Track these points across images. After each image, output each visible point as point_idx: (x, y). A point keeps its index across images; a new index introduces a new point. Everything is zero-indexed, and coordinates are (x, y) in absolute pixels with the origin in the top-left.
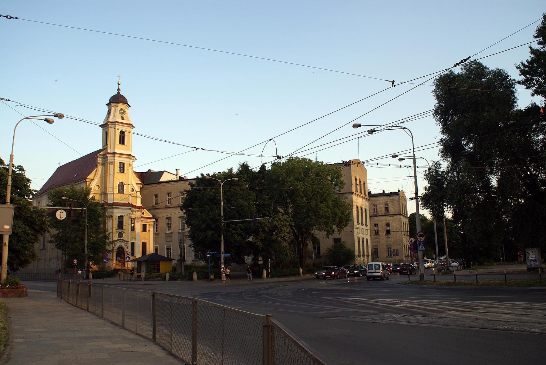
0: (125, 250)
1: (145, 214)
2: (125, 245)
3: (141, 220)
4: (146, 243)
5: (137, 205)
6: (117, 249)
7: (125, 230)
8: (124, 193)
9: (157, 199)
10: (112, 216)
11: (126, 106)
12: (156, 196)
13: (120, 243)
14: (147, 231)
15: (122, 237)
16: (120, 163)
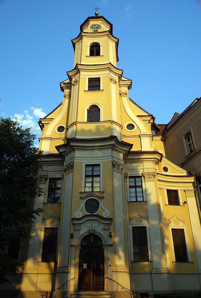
0: (104, 243)
2: (104, 230)
3: (159, 178)
4: (183, 230)
5: (142, 151)
8: (102, 119)
9: (191, 142)
10: (72, 164)
11: (101, 21)
12: (188, 136)
13: (89, 225)
16: (91, 80)
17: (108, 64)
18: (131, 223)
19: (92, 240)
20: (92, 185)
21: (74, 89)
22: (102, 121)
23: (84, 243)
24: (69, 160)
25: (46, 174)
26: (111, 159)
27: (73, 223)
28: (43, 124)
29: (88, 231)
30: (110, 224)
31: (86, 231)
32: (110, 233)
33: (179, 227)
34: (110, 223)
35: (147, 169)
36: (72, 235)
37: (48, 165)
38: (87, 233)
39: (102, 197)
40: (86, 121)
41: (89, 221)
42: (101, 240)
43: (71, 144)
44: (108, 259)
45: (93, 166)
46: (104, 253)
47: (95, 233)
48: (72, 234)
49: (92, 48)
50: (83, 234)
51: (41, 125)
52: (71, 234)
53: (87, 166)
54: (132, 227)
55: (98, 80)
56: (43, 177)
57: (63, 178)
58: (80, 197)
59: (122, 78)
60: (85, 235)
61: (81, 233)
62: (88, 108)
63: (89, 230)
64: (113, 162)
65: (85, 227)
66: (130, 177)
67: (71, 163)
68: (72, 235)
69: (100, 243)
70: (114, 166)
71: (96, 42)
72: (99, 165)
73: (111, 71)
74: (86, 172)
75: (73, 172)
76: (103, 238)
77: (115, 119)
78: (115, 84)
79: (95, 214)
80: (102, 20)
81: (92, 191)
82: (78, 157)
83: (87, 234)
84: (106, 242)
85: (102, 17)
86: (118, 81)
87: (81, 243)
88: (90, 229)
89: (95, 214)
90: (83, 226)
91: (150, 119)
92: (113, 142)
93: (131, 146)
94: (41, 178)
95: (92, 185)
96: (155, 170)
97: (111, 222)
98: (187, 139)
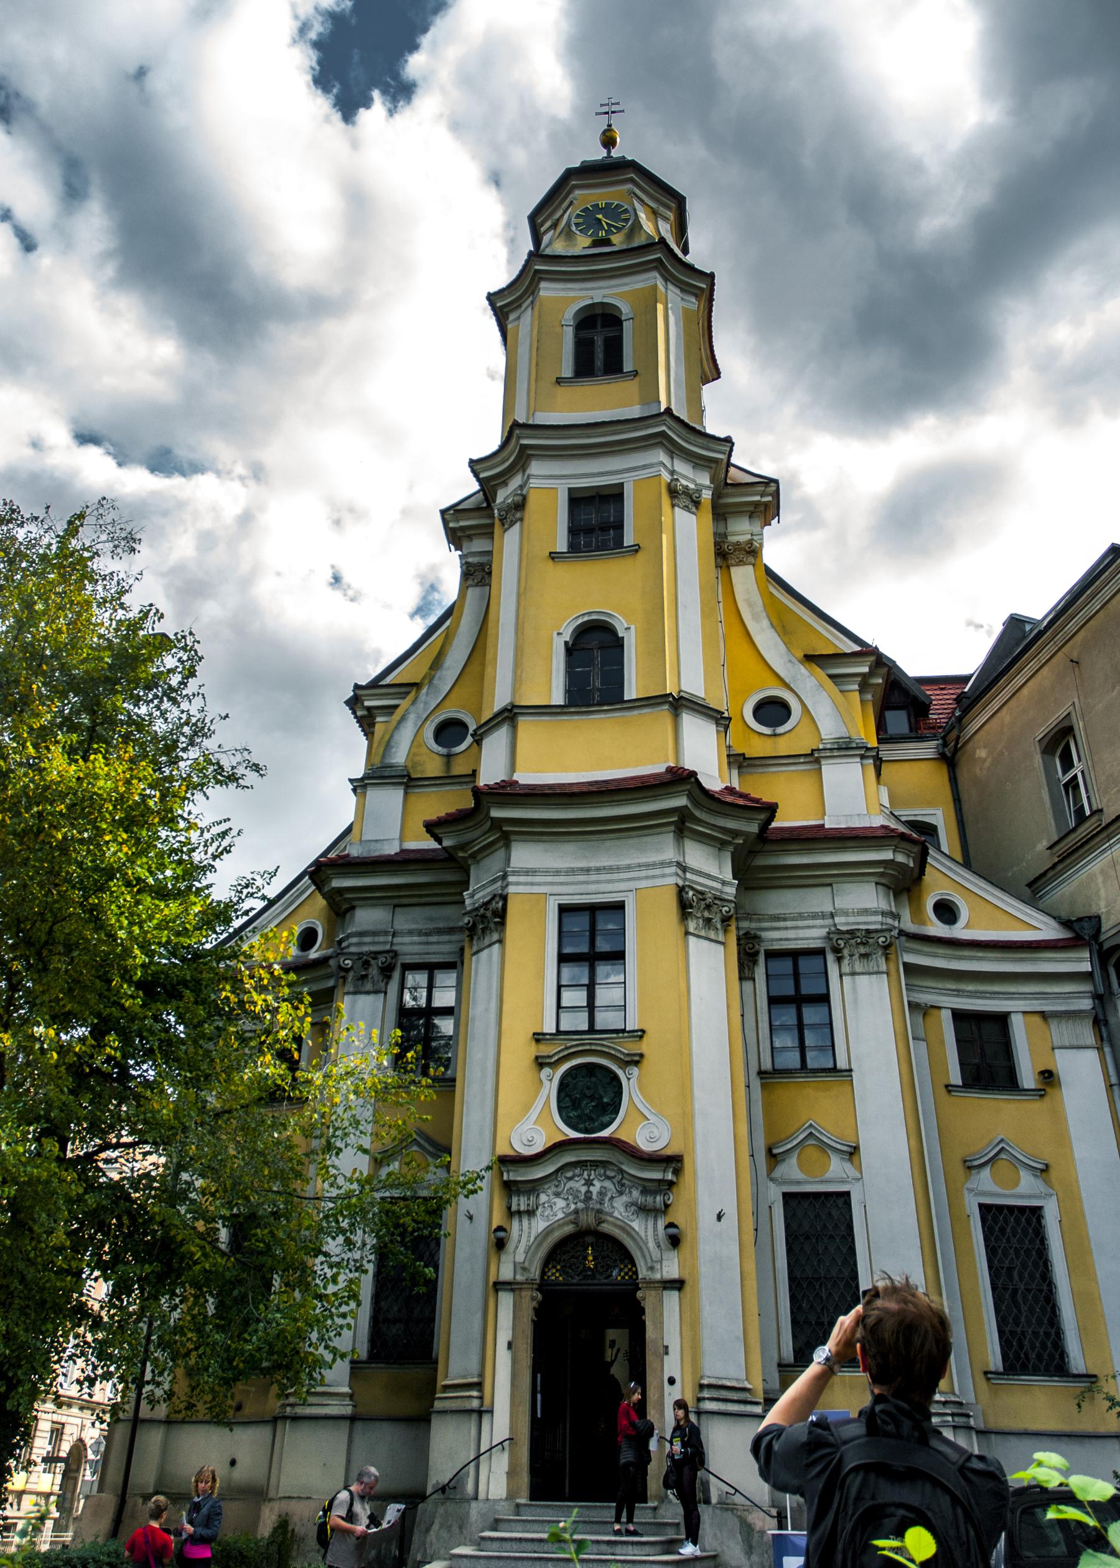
0: (643, 1273)
1: (964, 915)
2: (644, 1210)
4: (1036, 1213)
6: (551, 1259)
7: (640, 1034)
8: (631, 692)
11: (630, 186)
13: (578, 1185)
14: (1028, 1078)
15: (616, 1111)
17: (660, 419)
18: (779, 1172)
19: (591, 1258)
20: (591, 997)
21: (509, 543)
22: (634, 697)
23: (554, 1275)
24: (484, 887)
25: (388, 947)
26: (672, 880)
27: (505, 1177)
28: (369, 709)
29: (572, 1217)
30: (671, 1184)
31: (560, 1215)
32: (671, 1225)
33: (1022, 1197)
34: (670, 1176)
35: (846, 913)
36: (501, 1234)
37: (396, 901)
38: (567, 1223)
39: (635, 1055)
40: (558, 697)
41: (578, 1171)
42: (627, 1257)
43: (496, 813)
44: (661, 1350)
45: (593, 909)
46: (644, 1322)
47: (606, 1228)
48: (500, 1229)
49: (586, 334)
50: (548, 1231)
51: (359, 713)
52: (496, 1230)
53: (563, 909)
54: (786, 1195)
55: (613, 496)
56: (373, 962)
57: (462, 963)
58: (537, 1058)
59: (732, 470)
60: (557, 1235)
61: (539, 1224)
62: (567, 637)
63: (576, 1212)
64: (681, 890)
65: (557, 1195)
66: (771, 955)
67: (494, 897)
68: (501, 1234)
69: (626, 1274)
70: (684, 908)
71: (606, 300)
72: (620, 907)
73: (675, 450)
74: (565, 940)
75: (500, 941)
76: (641, 1249)
77: (694, 684)
78: (694, 509)
79: (605, 1133)
80: (632, 180)
81: (592, 1030)
82: (528, 872)
83: (569, 1229)
84: (652, 1268)
85: (633, 166)
86: (707, 495)
87: (543, 1273)
88: (581, 1205)
89: (605, 1133)
90: (550, 1192)
91: (866, 670)
92: (681, 801)
93: (771, 810)
94: (366, 964)
95: (591, 997)
96: (890, 921)
97: (677, 1172)
98: (1061, 757)
